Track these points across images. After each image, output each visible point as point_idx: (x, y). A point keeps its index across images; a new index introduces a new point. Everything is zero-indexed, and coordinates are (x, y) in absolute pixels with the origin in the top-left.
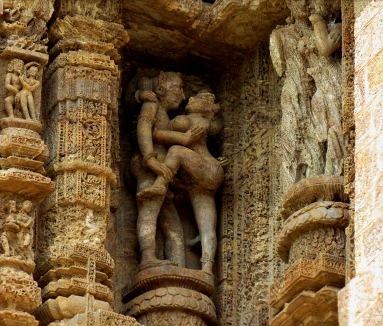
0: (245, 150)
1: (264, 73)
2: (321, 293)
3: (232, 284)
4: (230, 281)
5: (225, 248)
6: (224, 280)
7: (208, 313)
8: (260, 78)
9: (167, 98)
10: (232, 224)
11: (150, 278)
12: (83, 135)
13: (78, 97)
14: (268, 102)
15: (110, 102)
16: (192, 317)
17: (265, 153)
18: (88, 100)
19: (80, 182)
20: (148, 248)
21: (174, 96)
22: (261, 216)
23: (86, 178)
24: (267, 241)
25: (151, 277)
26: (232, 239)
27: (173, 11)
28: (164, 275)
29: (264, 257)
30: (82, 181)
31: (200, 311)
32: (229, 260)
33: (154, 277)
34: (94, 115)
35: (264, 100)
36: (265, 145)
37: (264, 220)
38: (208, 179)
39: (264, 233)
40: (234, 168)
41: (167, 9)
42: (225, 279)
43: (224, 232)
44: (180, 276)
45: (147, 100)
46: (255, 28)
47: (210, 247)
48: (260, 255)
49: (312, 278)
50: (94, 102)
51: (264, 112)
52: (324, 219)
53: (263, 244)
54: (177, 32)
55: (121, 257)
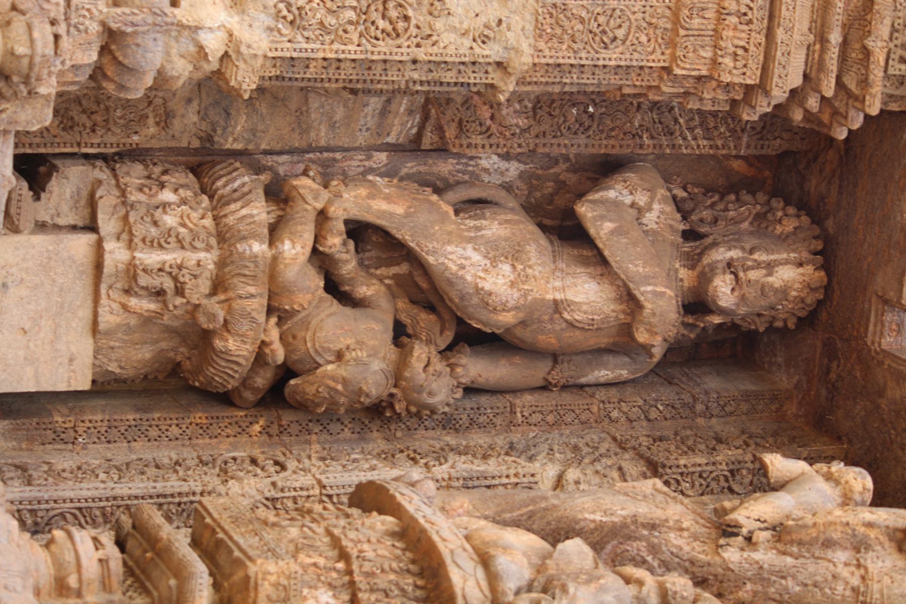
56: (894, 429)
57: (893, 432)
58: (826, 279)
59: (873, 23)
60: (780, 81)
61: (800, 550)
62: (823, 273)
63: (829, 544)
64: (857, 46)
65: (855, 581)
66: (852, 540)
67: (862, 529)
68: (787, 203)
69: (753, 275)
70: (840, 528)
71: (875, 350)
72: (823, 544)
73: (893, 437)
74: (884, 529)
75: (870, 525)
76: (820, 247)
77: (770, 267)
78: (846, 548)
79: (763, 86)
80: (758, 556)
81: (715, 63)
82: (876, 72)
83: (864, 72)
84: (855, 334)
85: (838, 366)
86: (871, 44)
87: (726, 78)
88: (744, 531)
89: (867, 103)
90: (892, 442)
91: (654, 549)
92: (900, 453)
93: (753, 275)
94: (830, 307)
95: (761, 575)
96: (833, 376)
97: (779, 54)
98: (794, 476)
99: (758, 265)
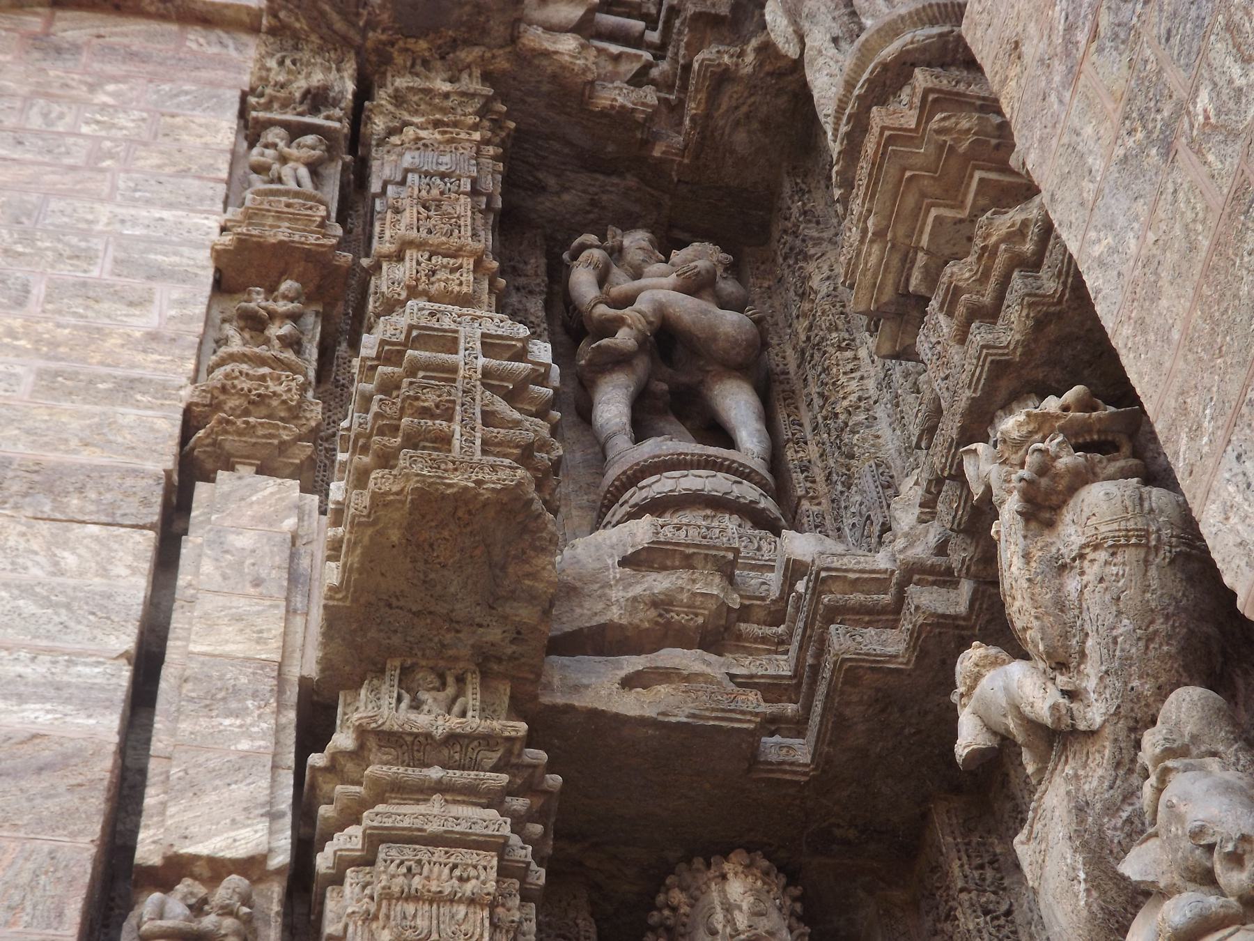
0: (798, 317)
1: (803, 194)
2: (935, 127)
3: (819, 504)
4: (813, 498)
5: (791, 455)
6: (800, 498)
7: (762, 505)
8: (796, 198)
9: (629, 258)
10: (801, 425)
11: (624, 473)
12: (419, 213)
13: (407, 171)
14: (818, 223)
15: (475, 174)
16: (727, 516)
17: (828, 278)
18: (427, 174)
19: (414, 263)
20: (615, 434)
21: (640, 252)
22: (840, 349)
23: (429, 259)
24: (862, 378)
25: (625, 468)
26: (806, 443)
27: (604, 113)
28: (654, 457)
29: (860, 399)
30: (419, 263)
31: (742, 500)
32: (804, 469)
33: (631, 468)
34: (442, 193)
35: (810, 221)
36: (825, 267)
37: (849, 354)
38: (726, 334)
39: (852, 371)
40: (789, 359)
41: (591, 108)
42: (803, 497)
43: (786, 433)
44: (686, 454)
45: (583, 247)
46: (766, 125)
47: (755, 440)
48: (853, 397)
49: (910, 130)
50: (443, 176)
51: (816, 234)
52: (910, 47)
53: (853, 385)
54: (631, 181)
55: (581, 508)
56: (903, 728)
57: (906, 731)
58: (738, 851)
59: (415, 730)
60: (492, 827)
61: (1074, 636)
62: (732, 855)
63: (1061, 605)
64: (446, 752)
65: (1102, 555)
66: (1049, 576)
67: (1033, 564)
68: (653, 907)
69: (741, 921)
70: (1038, 590)
71: (814, 770)
72: (1062, 611)
73: (913, 731)
74: (1029, 541)
75: (1027, 557)
76: (701, 860)
77: (729, 908)
78: (1061, 585)
79: (501, 848)
80: (1091, 683)
81: (472, 901)
82: (474, 726)
83: (476, 743)
84: (798, 802)
85: (839, 826)
86: (440, 731)
87: (491, 886)
88: (1063, 701)
89: (513, 734)
90: (919, 732)
91: (1111, 809)
92: (930, 717)
93: (741, 921)
94: (771, 845)
95: (1117, 670)
96: (852, 834)
97: (457, 829)
98: (979, 722)
99: (730, 921)
